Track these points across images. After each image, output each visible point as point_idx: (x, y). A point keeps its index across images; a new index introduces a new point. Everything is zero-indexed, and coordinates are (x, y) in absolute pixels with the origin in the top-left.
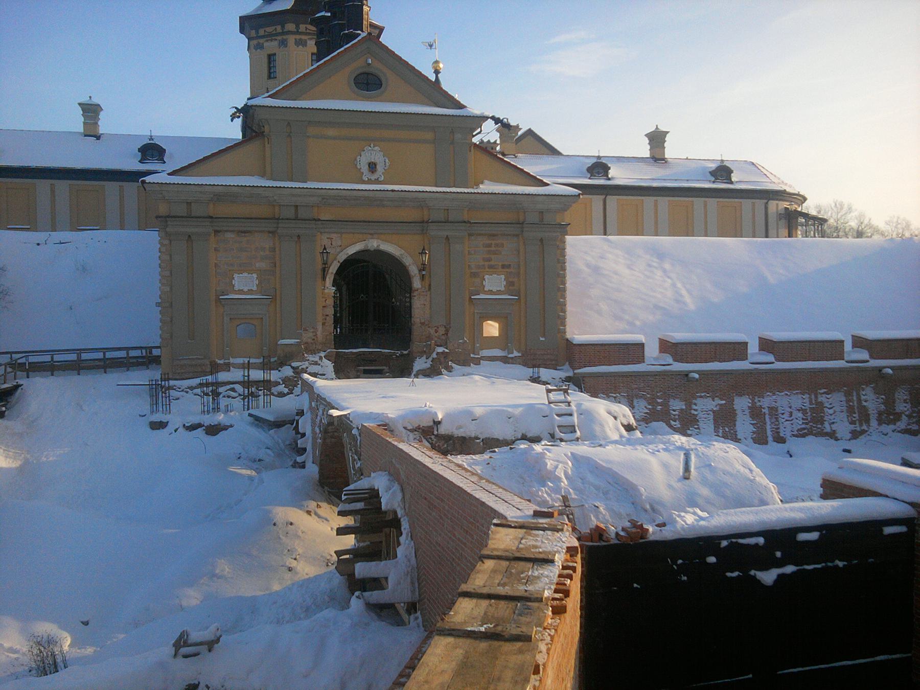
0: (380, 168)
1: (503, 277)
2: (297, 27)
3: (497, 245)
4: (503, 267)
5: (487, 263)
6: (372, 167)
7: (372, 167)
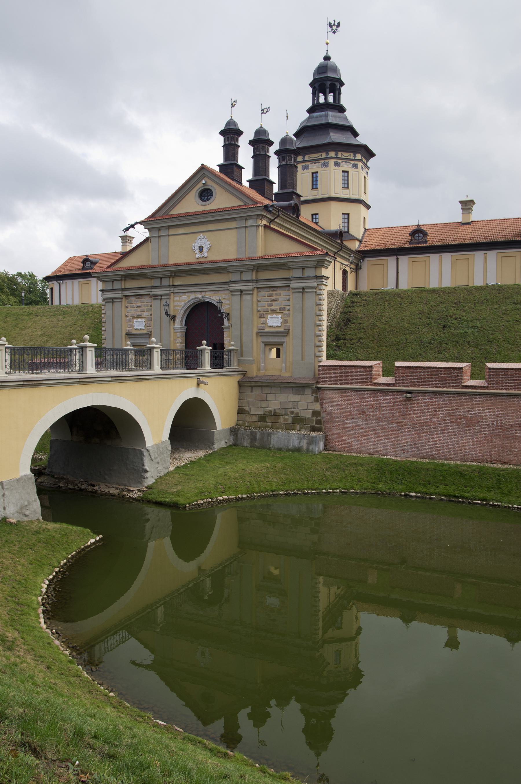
0: (205, 249)
1: (280, 316)
2: (304, 157)
3: (276, 295)
4: (280, 309)
5: (269, 308)
6: (201, 249)
7: (201, 249)
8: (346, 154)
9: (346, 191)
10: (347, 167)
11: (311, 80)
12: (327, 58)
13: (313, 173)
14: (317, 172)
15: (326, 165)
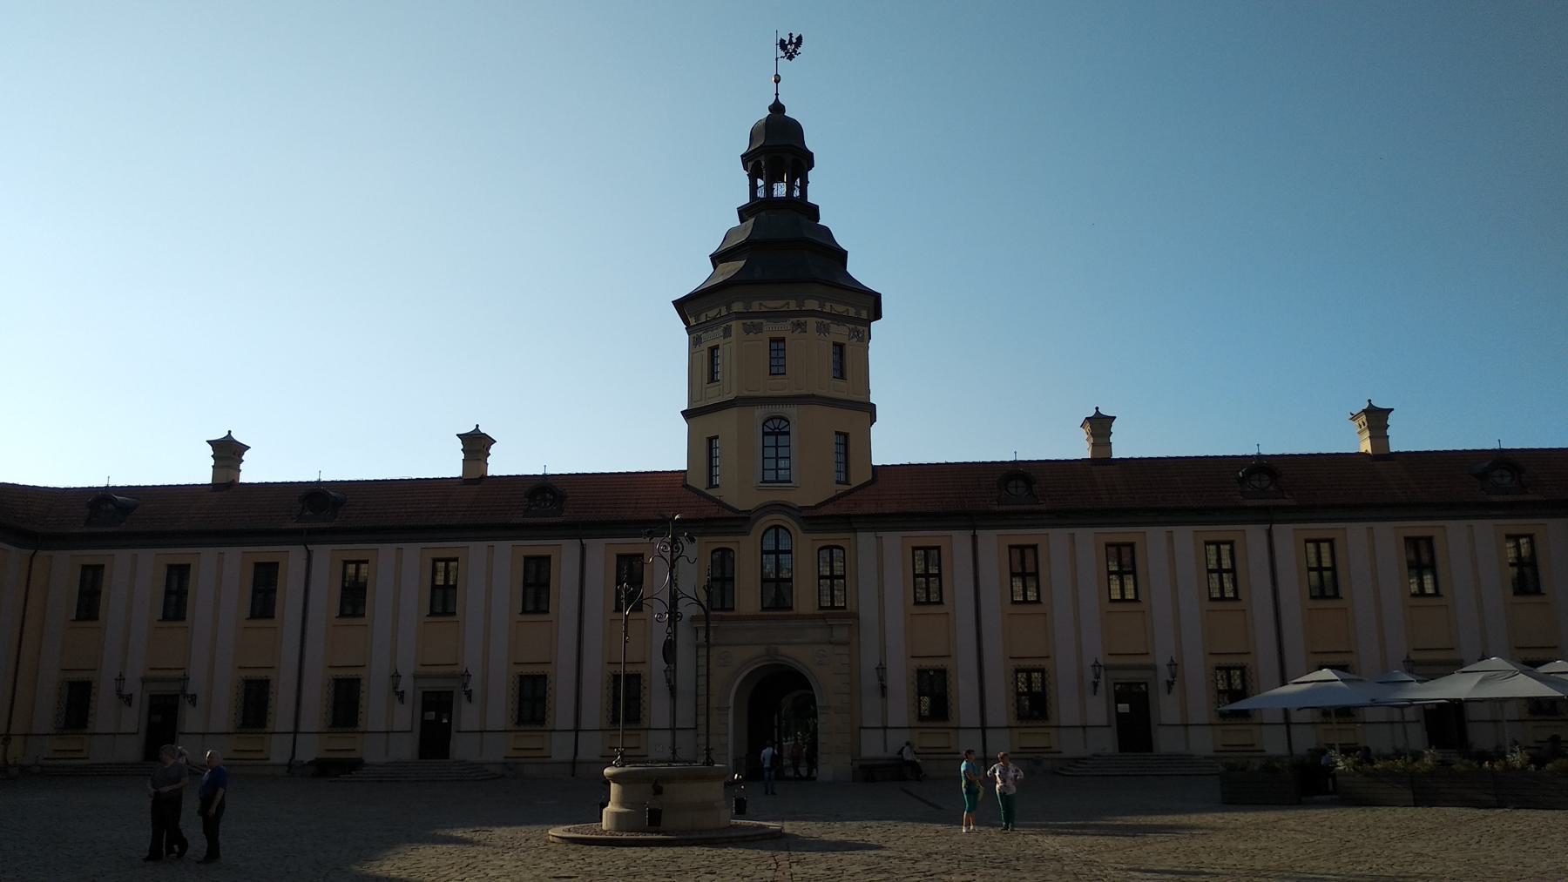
8: (840, 309)
9: (840, 383)
10: (840, 333)
11: (744, 148)
12: (777, 108)
13: (772, 340)
14: (783, 340)
15: (800, 326)
